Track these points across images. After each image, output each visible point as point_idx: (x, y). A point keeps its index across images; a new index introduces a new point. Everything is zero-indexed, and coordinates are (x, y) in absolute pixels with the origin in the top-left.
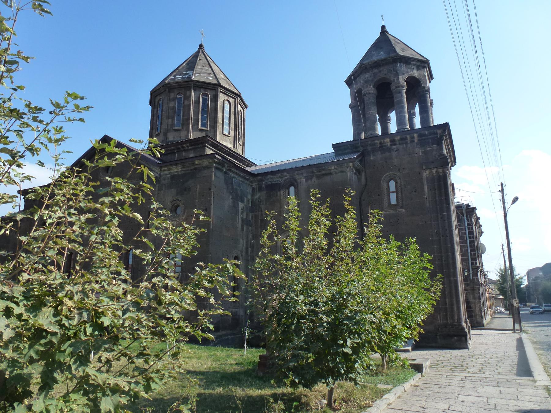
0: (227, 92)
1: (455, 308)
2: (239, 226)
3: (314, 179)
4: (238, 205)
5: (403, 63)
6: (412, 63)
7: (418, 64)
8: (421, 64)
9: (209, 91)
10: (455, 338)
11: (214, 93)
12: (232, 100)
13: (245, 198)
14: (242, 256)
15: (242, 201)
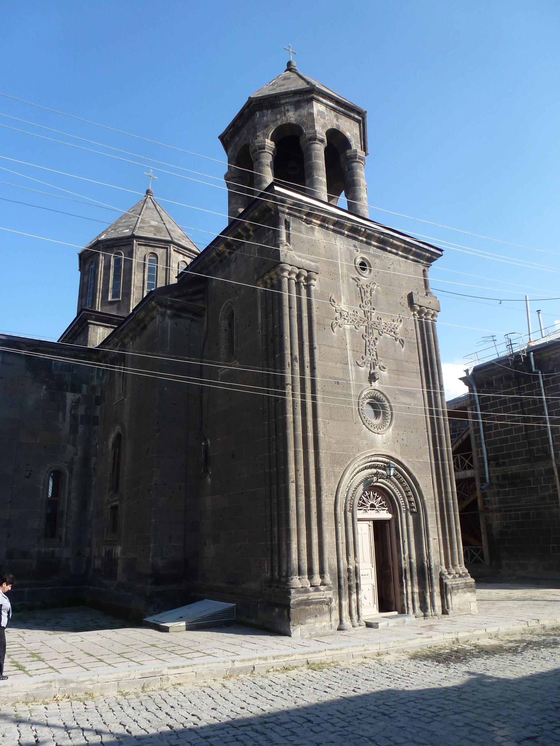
0: (147, 242)
1: (284, 547)
2: (66, 427)
3: (137, 340)
4: (64, 398)
5: (267, 108)
6: (283, 102)
7: (296, 99)
8: (301, 98)
9: (123, 247)
10: (277, 610)
11: (129, 248)
12: (160, 252)
13: (84, 386)
14: (71, 470)
15: (75, 389)
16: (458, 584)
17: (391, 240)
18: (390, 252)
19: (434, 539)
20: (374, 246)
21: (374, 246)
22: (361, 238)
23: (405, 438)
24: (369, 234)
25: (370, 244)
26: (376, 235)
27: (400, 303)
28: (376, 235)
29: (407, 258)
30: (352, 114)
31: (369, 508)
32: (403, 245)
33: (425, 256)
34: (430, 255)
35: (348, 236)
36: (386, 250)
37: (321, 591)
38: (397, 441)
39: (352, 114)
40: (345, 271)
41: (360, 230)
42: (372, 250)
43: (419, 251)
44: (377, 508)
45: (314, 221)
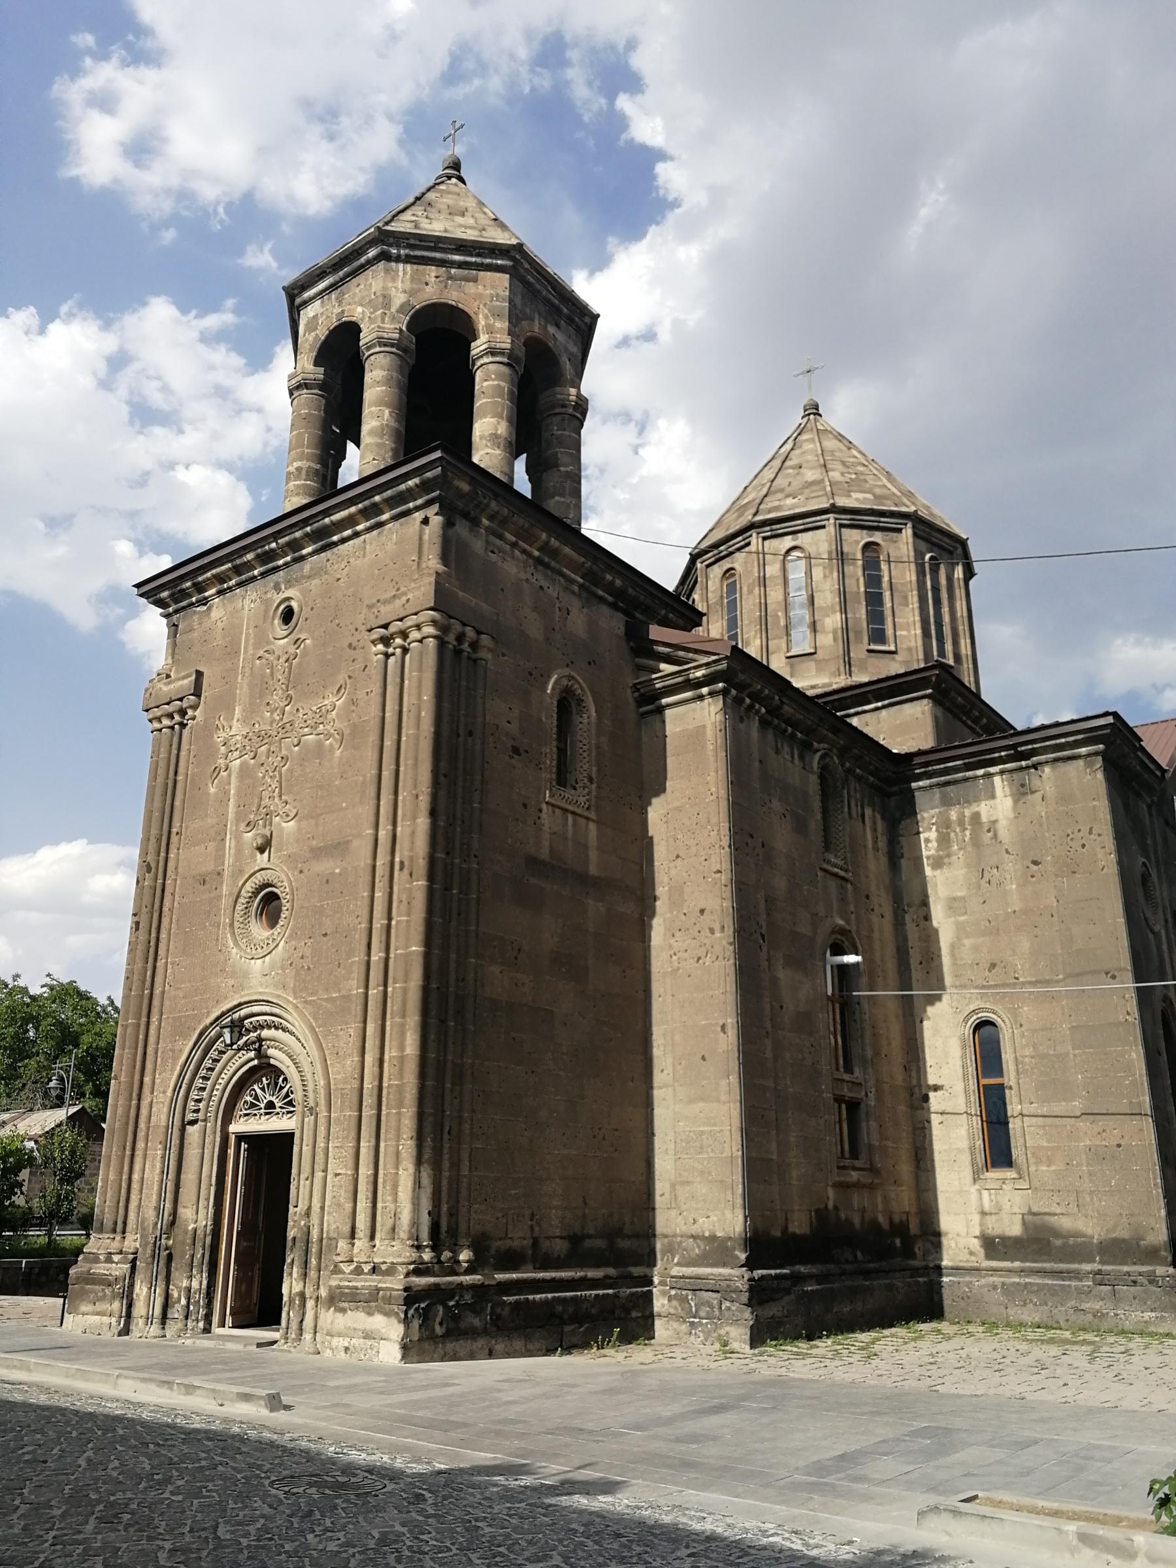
16: (357, 1288)
17: (327, 520)
18: (344, 541)
19: (337, 1175)
20: (312, 554)
21: (312, 554)
22: (281, 562)
23: (308, 952)
24: (288, 544)
25: (302, 558)
26: (298, 534)
27: (350, 645)
28: (298, 534)
29: (380, 525)
30: (363, 260)
31: (262, 1111)
32: (353, 509)
33: (409, 490)
34: (417, 480)
35: (263, 575)
36: (335, 544)
37: (113, 1262)
38: (291, 964)
39: (363, 260)
40: (251, 651)
41: (272, 550)
42: (307, 566)
43: (389, 493)
44: (278, 1110)
45: (206, 594)
